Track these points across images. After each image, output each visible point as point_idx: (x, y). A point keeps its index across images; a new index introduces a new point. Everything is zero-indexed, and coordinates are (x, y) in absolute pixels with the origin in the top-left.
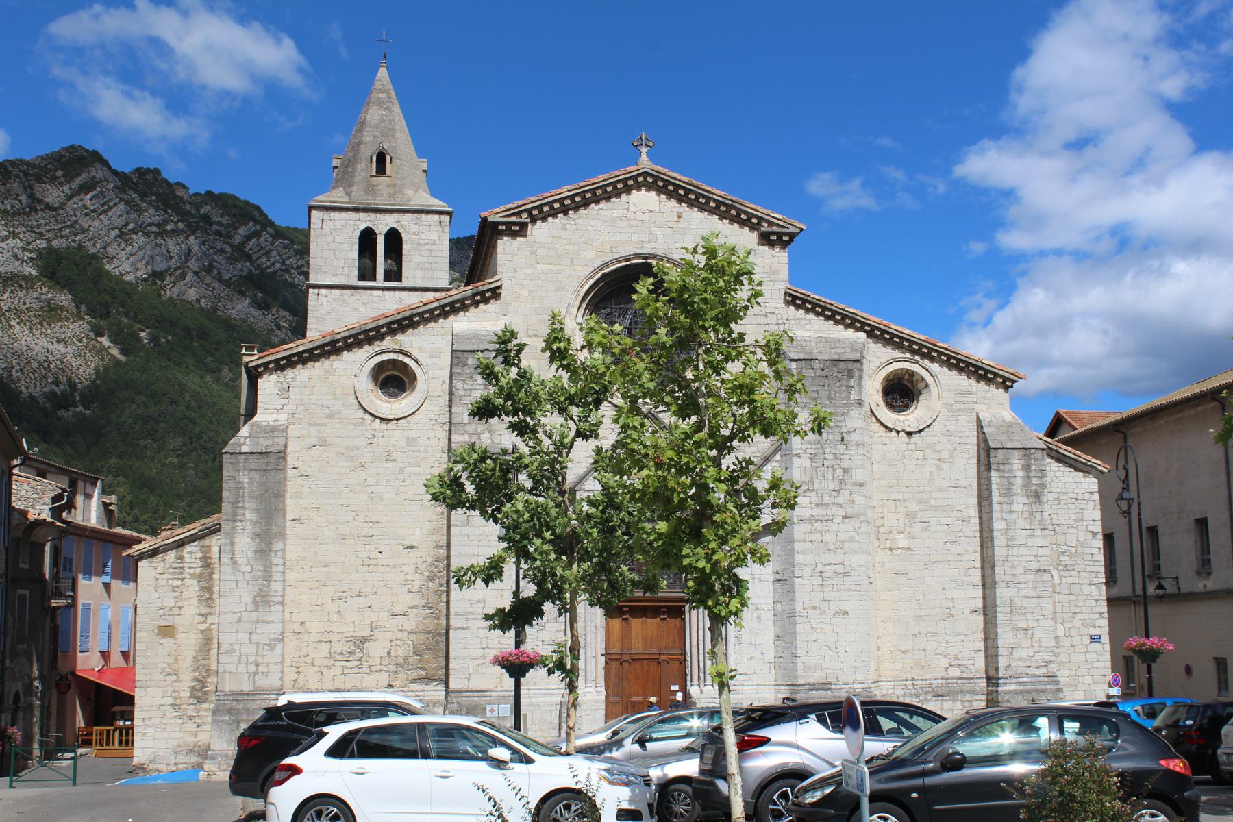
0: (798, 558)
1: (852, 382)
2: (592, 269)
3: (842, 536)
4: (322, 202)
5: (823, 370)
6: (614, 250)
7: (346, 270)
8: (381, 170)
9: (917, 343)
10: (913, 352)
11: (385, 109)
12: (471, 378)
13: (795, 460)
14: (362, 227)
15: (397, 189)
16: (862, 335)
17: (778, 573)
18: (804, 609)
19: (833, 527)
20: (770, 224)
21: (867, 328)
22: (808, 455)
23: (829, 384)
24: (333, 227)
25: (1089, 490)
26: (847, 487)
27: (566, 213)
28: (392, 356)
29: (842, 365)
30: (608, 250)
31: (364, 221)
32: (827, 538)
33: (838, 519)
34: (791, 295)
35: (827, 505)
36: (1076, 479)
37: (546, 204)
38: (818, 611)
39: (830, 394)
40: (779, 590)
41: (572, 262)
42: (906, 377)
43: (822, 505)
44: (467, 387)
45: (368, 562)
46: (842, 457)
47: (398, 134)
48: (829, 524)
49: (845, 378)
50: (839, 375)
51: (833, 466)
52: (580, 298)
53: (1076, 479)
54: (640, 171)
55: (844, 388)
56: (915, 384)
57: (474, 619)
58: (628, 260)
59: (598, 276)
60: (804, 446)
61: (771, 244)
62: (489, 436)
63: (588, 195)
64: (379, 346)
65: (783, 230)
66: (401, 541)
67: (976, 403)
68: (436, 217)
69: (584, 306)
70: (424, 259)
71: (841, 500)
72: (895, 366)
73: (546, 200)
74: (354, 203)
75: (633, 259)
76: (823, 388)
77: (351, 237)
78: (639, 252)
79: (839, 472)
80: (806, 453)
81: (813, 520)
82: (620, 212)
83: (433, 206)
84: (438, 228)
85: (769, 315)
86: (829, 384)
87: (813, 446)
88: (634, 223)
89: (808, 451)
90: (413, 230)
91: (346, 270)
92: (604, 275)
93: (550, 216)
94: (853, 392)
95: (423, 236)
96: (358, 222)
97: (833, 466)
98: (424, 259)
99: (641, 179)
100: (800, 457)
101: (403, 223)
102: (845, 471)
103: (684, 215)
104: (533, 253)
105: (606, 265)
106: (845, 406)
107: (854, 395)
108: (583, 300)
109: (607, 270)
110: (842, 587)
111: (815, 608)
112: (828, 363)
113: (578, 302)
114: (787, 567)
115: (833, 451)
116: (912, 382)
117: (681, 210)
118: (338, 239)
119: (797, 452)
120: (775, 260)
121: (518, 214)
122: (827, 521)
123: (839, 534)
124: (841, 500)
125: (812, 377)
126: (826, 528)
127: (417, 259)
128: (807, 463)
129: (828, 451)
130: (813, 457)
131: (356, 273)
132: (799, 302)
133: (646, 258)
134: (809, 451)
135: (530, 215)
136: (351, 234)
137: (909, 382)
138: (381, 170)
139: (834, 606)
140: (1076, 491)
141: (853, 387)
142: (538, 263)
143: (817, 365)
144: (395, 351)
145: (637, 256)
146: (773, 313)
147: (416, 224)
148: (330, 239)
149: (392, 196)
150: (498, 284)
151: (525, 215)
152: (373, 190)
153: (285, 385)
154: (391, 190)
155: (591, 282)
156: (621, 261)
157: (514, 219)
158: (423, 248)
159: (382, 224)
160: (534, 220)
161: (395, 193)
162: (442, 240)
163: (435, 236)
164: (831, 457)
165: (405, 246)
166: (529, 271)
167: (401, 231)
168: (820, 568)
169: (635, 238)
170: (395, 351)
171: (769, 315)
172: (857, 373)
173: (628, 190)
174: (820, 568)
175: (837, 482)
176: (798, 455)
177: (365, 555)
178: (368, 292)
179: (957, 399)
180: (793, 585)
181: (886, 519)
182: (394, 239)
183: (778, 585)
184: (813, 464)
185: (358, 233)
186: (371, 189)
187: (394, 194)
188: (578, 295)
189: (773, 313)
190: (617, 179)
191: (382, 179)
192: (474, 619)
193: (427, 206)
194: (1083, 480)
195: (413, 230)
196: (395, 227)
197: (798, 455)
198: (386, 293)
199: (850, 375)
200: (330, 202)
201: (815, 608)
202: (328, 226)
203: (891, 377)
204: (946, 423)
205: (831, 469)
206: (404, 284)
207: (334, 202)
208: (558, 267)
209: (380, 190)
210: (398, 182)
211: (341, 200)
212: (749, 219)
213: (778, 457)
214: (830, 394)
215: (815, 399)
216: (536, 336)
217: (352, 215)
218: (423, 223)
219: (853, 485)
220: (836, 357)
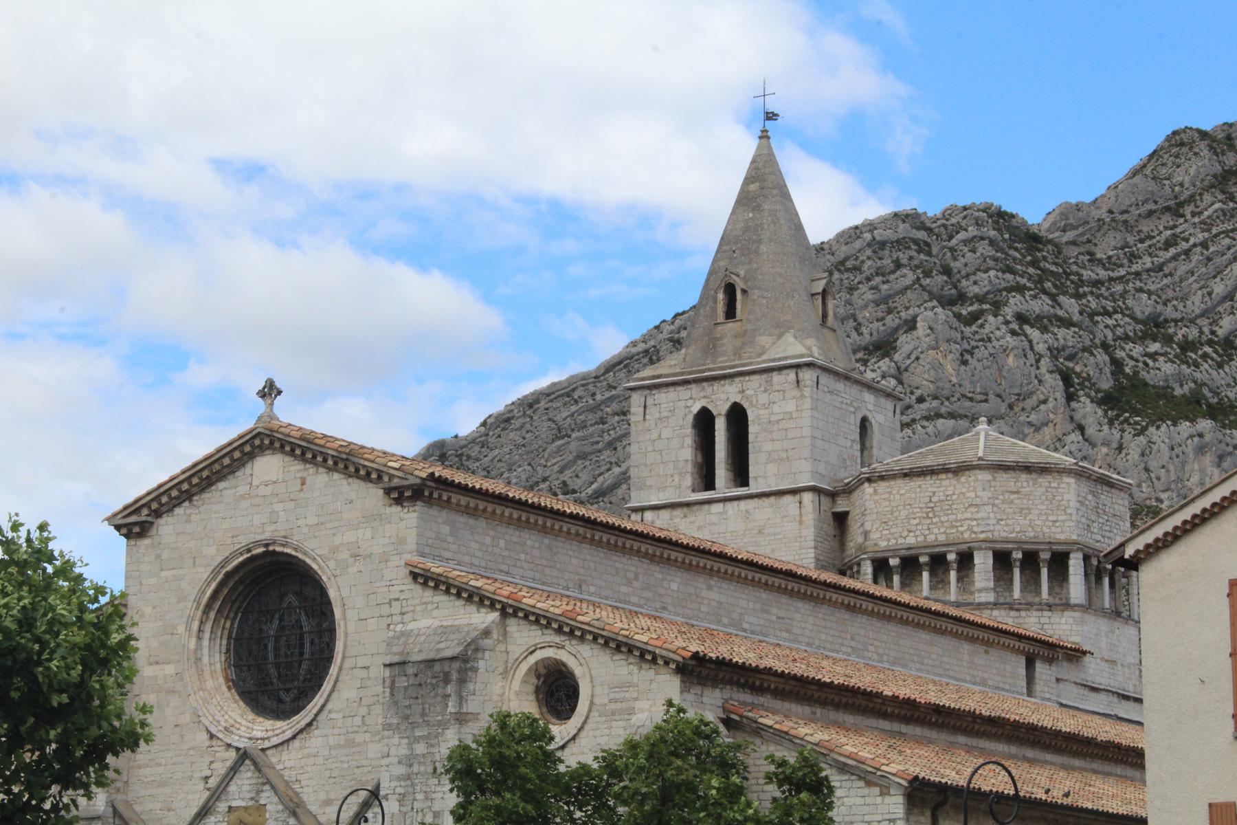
1: (450, 689)
2: (212, 568)
4: (643, 379)
5: (416, 675)
6: (235, 540)
7: (676, 478)
8: (730, 313)
10: (559, 631)
11: (753, 209)
14: (696, 409)
15: (746, 338)
16: (495, 616)
20: (391, 477)
22: (397, 796)
23: (422, 696)
24: (657, 415)
25: (887, 817)
29: (437, 667)
30: (229, 541)
31: (693, 401)
34: (411, 573)
36: (868, 800)
39: (424, 709)
41: (195, 562)
46: (434, 796)
47: (763, 248)
49: (441, 684)
50: (434, 681)
51: (422, 810)
52: (202, 608)
53: (868, 800)
54: (254, 433)
55: (439, 699)
58: (249, 551)
59: (221, 577)
60: (393, 784)
61: (399, 501)
63: (205, 474)
65: (405, 483)
67: (636, 699)
68: (791, 375)
69: (212, 615)
70: (778, 446)
72: (539, 655)
73: (162, 490)
74: (683, 374)
75: (255, 547)
76: (416, 701)
77: (682, 427)
78: (258, 538)
82: (243, 489)
83: (786, 358)
84: (796, 393)
85: (394, 603)
86: (422, 696)
87: (403, 783)
88: (256, 501)
90: (761, 402)
91: (676, 478)
92: (228, 575)
93: (175, 506)
94: (450, 704)
95: (776, 409)
96: (690, 403)
97: (422, 810)
98: (778, 446)
99: (257, 442)
101: (751, 394)
103: (308, 481)
104: (158, 557)
105: (226, 561)
106: (440, 724)
107: (451, 708)
108: (208, 607)
109: (229, 567)
112: (422, 666)
113: (199, 613)
115: (424, 789)
117: (304, 474)
118: (666, 433)
120: (403, 525)
121: (137, 511)
125: (405, 687)
127: (768, 447)
129: (418, 788)
131: (688, 481)
133: (267, 545)
134: (399, 790)
136: (681, 423)
138: (730, 313)
140: (867, 818)
141: (449, 696)
142: (162, 570)
143: (410, 670)
145: (257, 543)
146: (397, 599)
147: (765, 391)
148: (654, 436)
149: (738, 353)
151: (145, 511)
152: (714, 347)
154: (738, 343)
155: (214, 585)
156: (241, 554)
157: (133, 519)
158: (775, 428)
159: (720, 399)
160: (158, 514)
161: (743, 345)
162: (801, 411)
163: (790, 406)
164: (420, 796)
165: (751, 429)
166: (153, 581)
167: (746, 405)
169: (257, 520)
171: (394, 603)
172: (454, 676)
173: (251, 456)
178: (706, 507)
179: (612, 696)
182: (738, 416)
184: (402, 809)
185: (690, 419)
186: (712, 346)
187: (741, 347)
188: (199, 604)
189: (397, 599)
191: (731, 326)
193: (780, 359)
194: (879, 800)
195: (761, 402)
196: (738, 401)
198: (729, 505)
199: (447, 680)
200: (654, 377)
202: (653, 413)
203: (543, 671)
204: (597, 733)
205: (420, 814)
206: (754, 488)
207: (659, 377)
208: (181, 571)
209: (723, 345)
210: (750, 327)
211: (678, 370)
212: (368, 474)
214: (424, 709)
216: (157, 663)
217: (682, 392)
218: (777, 388)
220: (431, 656)
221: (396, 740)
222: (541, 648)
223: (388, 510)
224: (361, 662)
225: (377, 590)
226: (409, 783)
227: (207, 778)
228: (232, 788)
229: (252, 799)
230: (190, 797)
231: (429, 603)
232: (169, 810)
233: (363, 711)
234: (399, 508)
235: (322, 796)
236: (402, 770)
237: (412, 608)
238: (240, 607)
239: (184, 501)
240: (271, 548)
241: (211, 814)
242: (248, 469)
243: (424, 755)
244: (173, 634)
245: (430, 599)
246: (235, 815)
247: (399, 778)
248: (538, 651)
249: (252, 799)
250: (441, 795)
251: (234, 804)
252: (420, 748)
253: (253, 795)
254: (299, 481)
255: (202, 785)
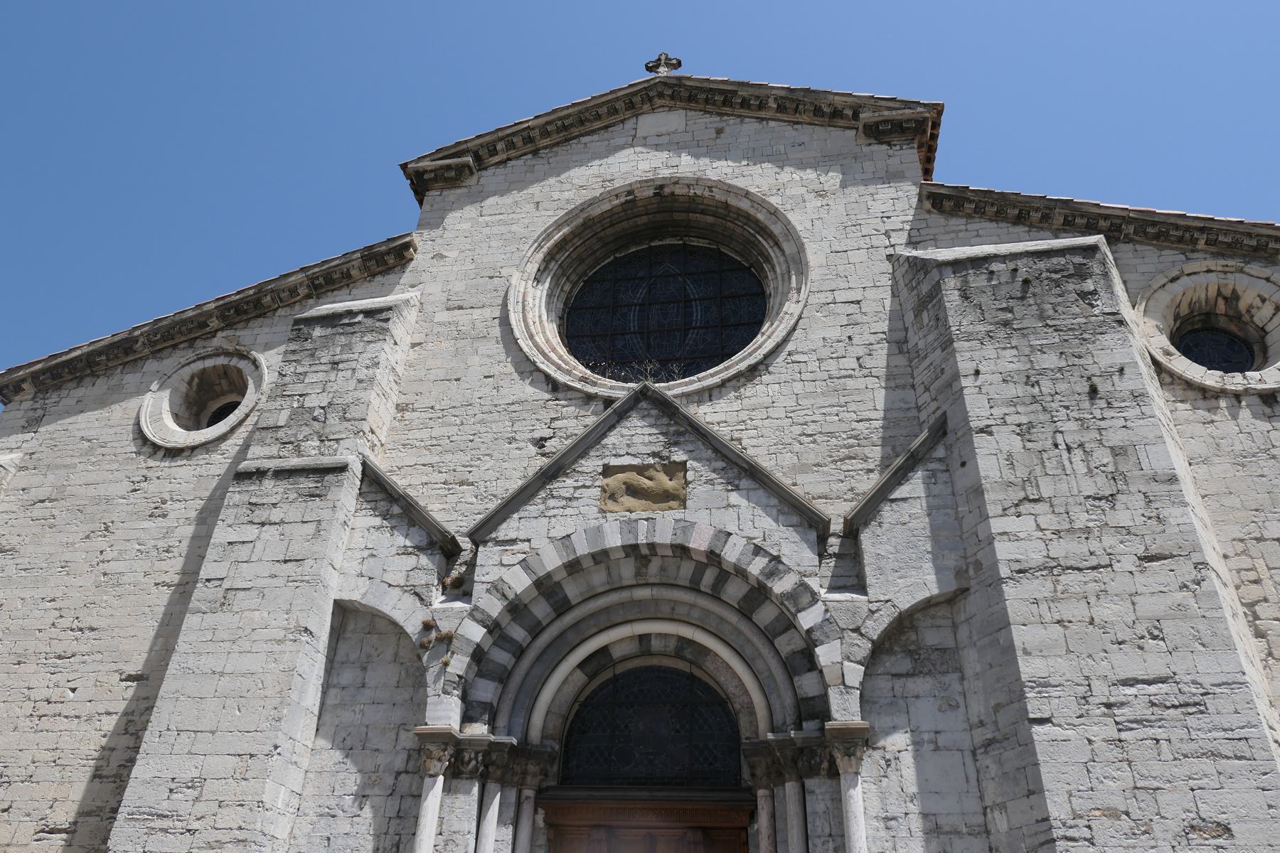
0: (1028, 668)
3: (1150, 606)
9: (1226, 233)
12: (312, 355)
13: (979, 440)
17: (982, 724)
18: (1076, 816)
19: (1119, 583)
21: (1102, 223)
26: (1133, 489)
27: (535, 153)
28: (222, 361)
32: (1104, 611)
33: (1129, 563)
35: (1088, 530)
37: (501, 139)
38: (1125, 823)
40: (993, 769)
42: (1221, 306)
43: (1071, 531)
44: (300, 370)
45: (44, 708)
46: (1102, 424)
48: (1104, 574)
56: (1246, 318)
57: (165, 831)
58: (630, 193)
60: (998, 412)
62: (318, 443)
64: (203, 347)
66: (121, 666)
71: (1122, 517)
73: (500, 134)
79: (1103, 456)
80: (1005, 423)
81: (1052, 568)
87: (1020, 409)
89: (1009, 419)
100: (991, 434)
102: (1117, 452)
103: (727, 130)
110: (1187, 747)
111: (1112, 813)
113: (540, 256)
114: (1002, 698)
115: (1075, 414)
116: (1237, 317)
117: (721, 125)
119: (982, 424)
122: (1094, 568)
123: (1136, 599)
124: (1122, 517)
126: (1093, 587)
128: (1008, 440)
130: (1025, 431)
132: (948, 204)
135: (478, 158)
137: (1231, 318)
139: (1175, 806)
141: (1094, 292)
144: (227, 354)
150: (408, 239)
153: (40, 412)
155: (566, 230)
164: (1073, 426)
168: (1101, 691)
170: (227, 354)
174: (1101, 691)
175: (1101, 480)
176: (986, 430)
177: (46, 693)
180: (1028, 746)
181: (1268, 583)
183: (986, 761)
184: (1029, 445)
190: (614, 96)
192: (165, 831)
197: (986, 430)
201: (1112, 813)
203: (1184, 310)
213: (940, 452)
214: (1042, 311)
215: (1006, 324)
216: (460, 308)
219: (1147, 482)
221: (990, 350)
222: (1188, 275)
223: (865, 149)
224: (841, 296)
225: (859, 222)
226: (1037, 407)
227: (540, 443)
228: (611, 439)
229: (654, 455)
230: (505, 465)
231: (961, 231)
232: (462, 484)
233: (861, 351)
234: (885, 147)
235: (788, 459)
236: (1020, 390)
237: (932, 237)
238: (585, 274)
239: (525, 154)
240: (667, 191)
241: (566, 475)
242: (630, 124)
243: (1060, 369)
244: (491, 278)
245: (963, 227)
246: (614, 481)
247: (1012, 403)
248: (1184, 279)
249: (654, 455)
250: (1122, 422)
251: (614, 462)
252: (1050, 360)
253: (656, 449)
254: (713, 131)
255: (533, 450)
